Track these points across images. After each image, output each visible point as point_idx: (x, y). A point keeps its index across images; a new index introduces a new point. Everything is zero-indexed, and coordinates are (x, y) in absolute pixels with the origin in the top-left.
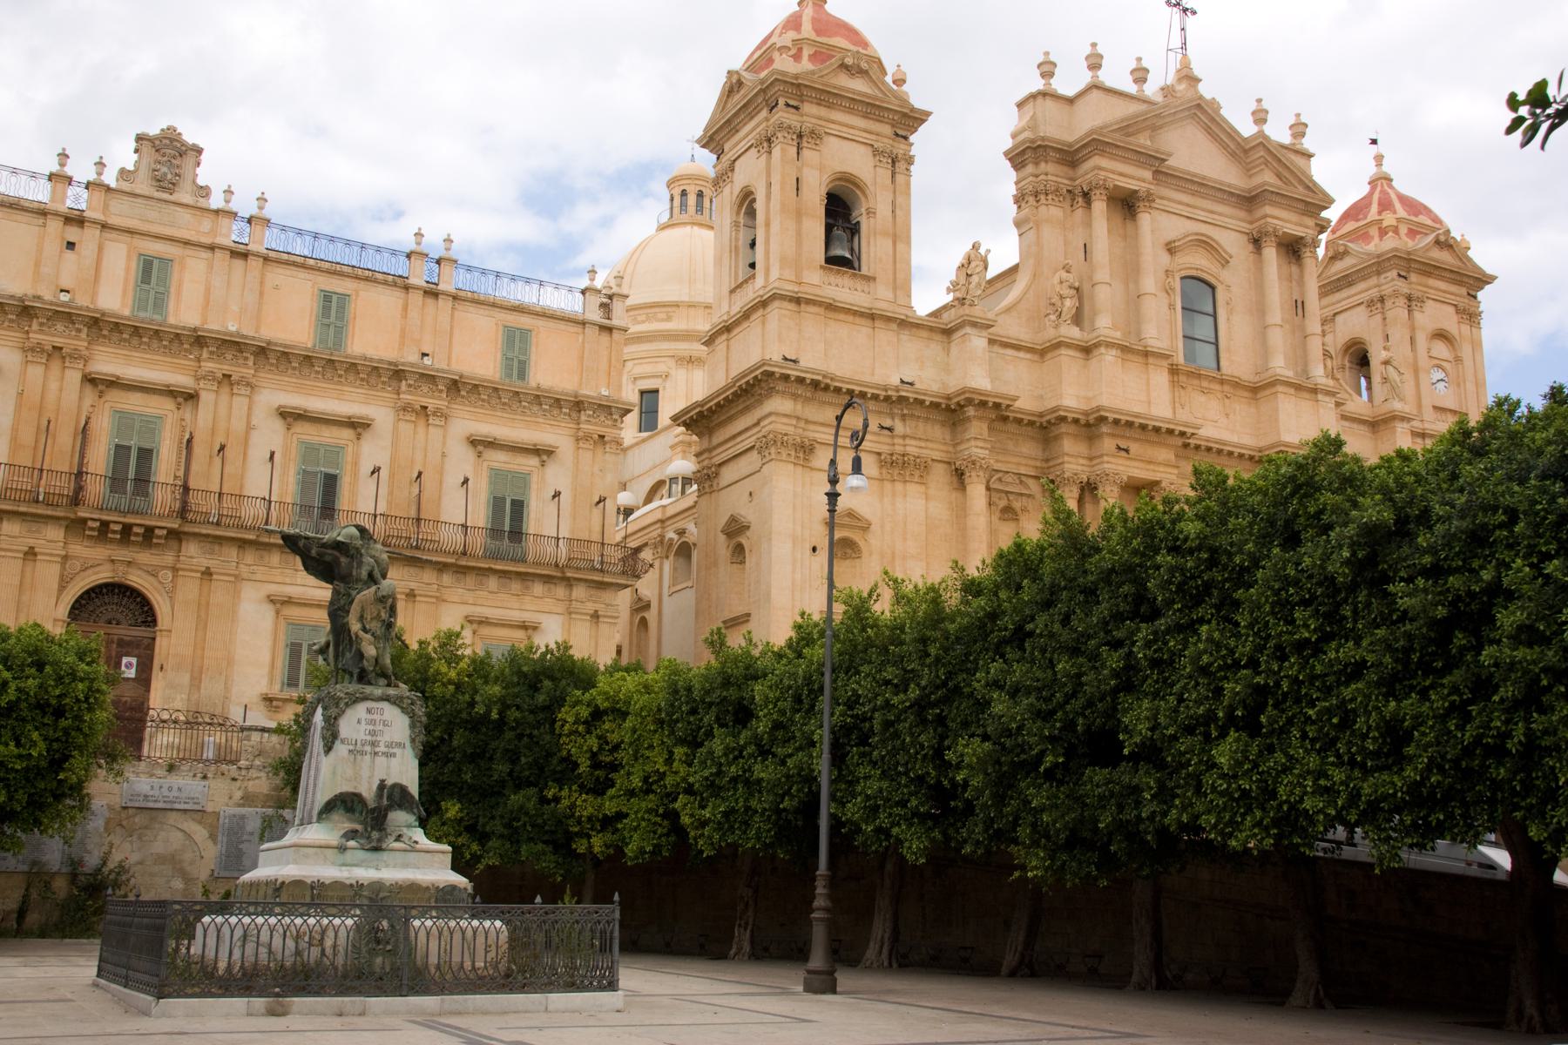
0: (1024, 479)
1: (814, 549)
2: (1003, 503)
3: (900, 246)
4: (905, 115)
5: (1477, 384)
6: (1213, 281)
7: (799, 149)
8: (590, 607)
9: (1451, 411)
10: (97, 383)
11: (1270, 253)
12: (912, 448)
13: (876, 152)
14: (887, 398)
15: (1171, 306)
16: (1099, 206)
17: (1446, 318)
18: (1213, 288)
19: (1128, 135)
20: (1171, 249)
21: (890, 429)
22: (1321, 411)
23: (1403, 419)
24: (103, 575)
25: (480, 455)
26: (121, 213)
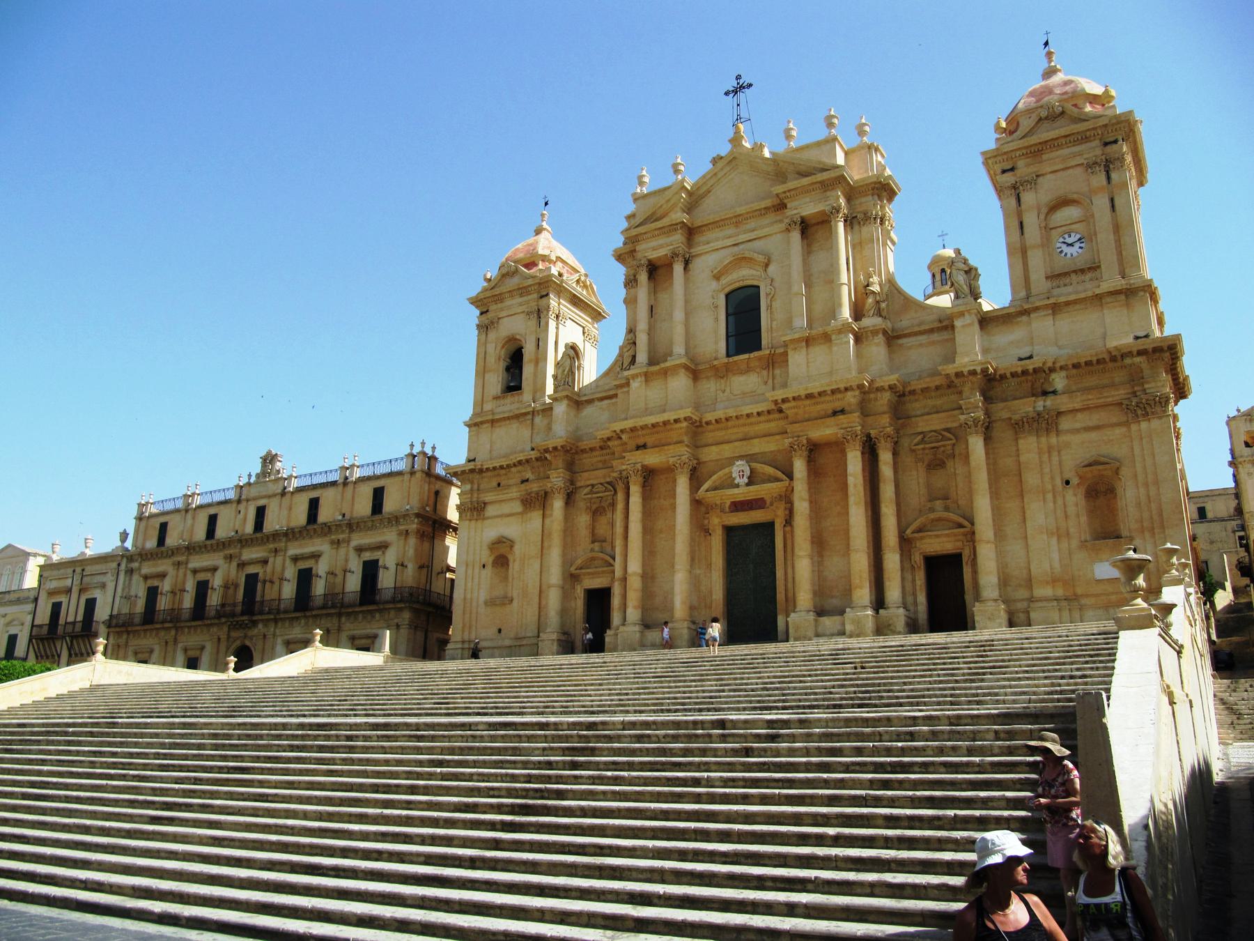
0: (606, 485)
1: (484, 566)
2: (594, 507)
3: (540, 365)
4: (540, 284)
5: (1117, 228)
6: (755, 283)
7: (487, 334)
8: (396, 621)
9: (1075, 272)
10: (242, 565)
11: (796, 236)
12: (535, 487)
13: (528, 314)
14: (515, 465)
15: (717, 319)
16: (643, 277)
17: (1074, 181)
18: (758, 287)
19: (656, 220)
20: (717, 277)
21: (527, 480)
22: (835, 349)
23: (962, 314)
24: (238, 643)
25: (359, 556)
26: (254, 492)
